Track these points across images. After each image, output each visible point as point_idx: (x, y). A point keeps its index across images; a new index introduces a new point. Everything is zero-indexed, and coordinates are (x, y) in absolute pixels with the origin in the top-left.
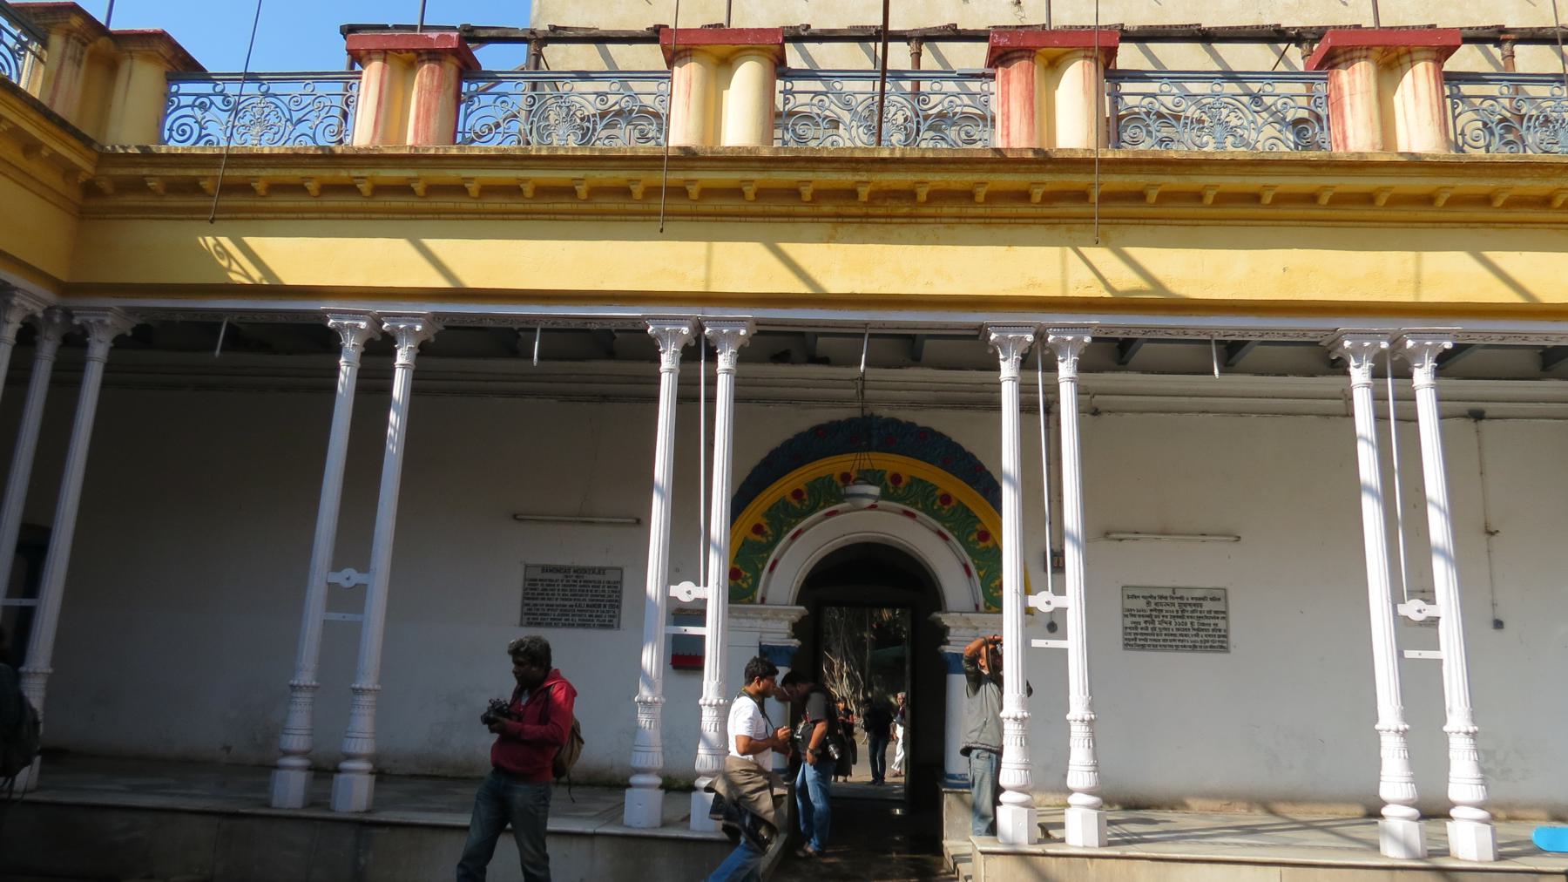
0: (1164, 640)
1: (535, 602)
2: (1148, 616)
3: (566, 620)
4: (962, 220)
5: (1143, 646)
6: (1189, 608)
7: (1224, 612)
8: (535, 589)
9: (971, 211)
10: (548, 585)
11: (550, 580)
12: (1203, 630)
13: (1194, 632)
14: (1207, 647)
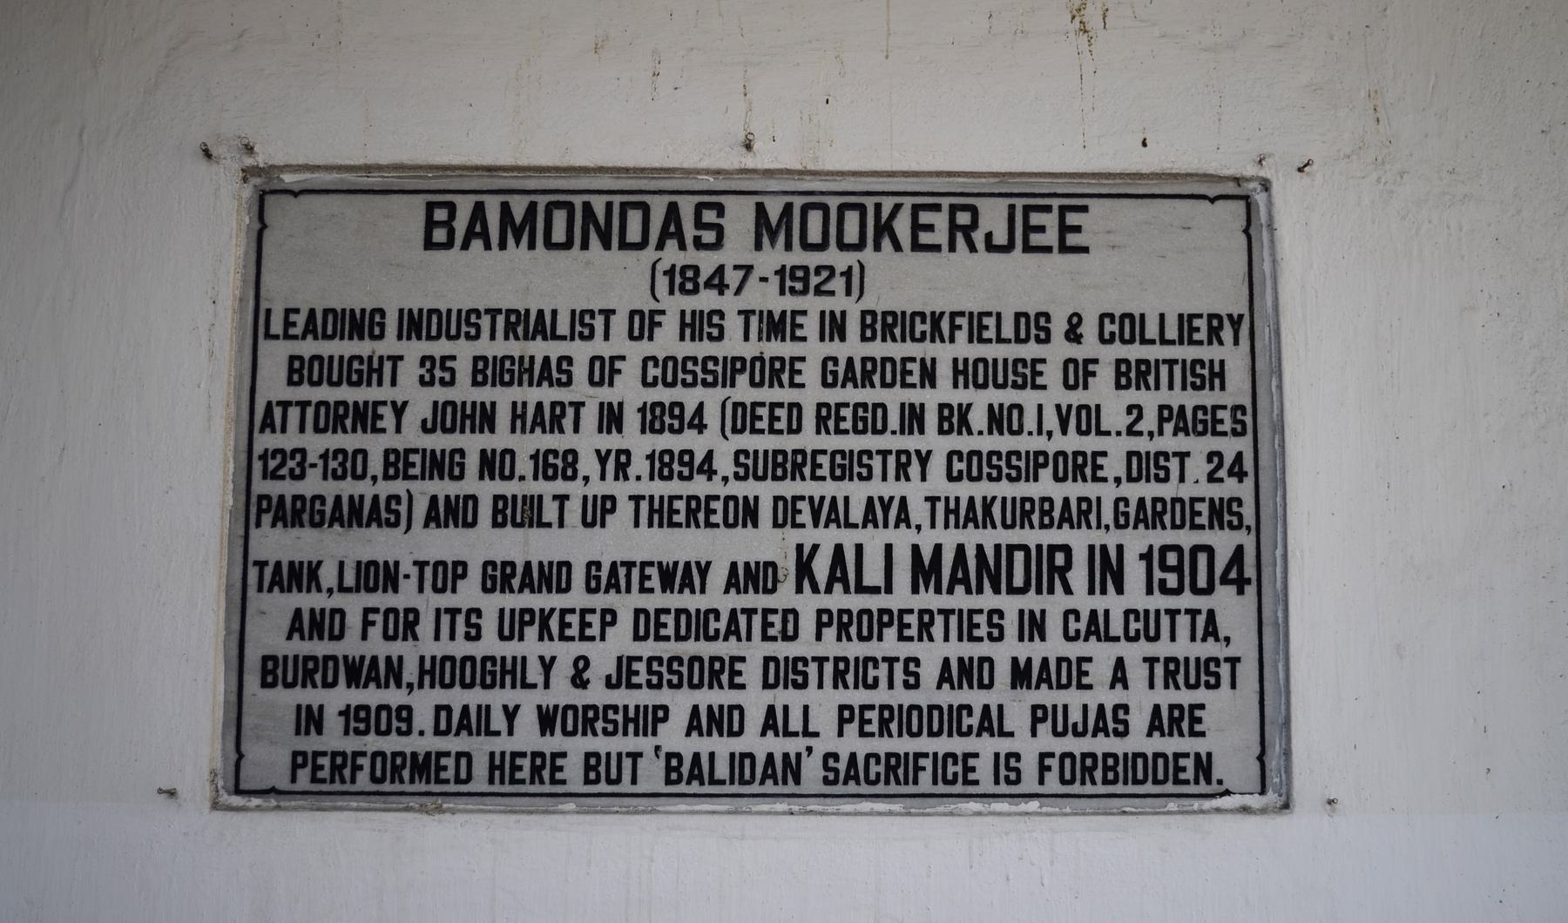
1: (379, 544)
3: (722, 721)
8: (365, 417)
10: (487, 371)
11: (521, 323)
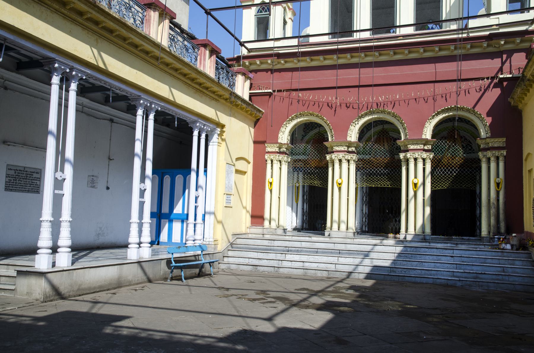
0: (19, 188)
2: (15, 178)
4: (57, 12)
5: (12, 189)
6: (29, 176)
7: (39, 178)
9: (63, 10)
12: (32, 184)
13: (29, 185)
14: (32, 191)
